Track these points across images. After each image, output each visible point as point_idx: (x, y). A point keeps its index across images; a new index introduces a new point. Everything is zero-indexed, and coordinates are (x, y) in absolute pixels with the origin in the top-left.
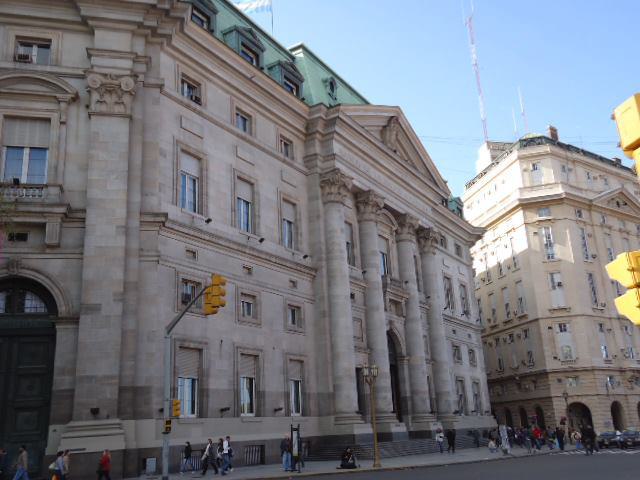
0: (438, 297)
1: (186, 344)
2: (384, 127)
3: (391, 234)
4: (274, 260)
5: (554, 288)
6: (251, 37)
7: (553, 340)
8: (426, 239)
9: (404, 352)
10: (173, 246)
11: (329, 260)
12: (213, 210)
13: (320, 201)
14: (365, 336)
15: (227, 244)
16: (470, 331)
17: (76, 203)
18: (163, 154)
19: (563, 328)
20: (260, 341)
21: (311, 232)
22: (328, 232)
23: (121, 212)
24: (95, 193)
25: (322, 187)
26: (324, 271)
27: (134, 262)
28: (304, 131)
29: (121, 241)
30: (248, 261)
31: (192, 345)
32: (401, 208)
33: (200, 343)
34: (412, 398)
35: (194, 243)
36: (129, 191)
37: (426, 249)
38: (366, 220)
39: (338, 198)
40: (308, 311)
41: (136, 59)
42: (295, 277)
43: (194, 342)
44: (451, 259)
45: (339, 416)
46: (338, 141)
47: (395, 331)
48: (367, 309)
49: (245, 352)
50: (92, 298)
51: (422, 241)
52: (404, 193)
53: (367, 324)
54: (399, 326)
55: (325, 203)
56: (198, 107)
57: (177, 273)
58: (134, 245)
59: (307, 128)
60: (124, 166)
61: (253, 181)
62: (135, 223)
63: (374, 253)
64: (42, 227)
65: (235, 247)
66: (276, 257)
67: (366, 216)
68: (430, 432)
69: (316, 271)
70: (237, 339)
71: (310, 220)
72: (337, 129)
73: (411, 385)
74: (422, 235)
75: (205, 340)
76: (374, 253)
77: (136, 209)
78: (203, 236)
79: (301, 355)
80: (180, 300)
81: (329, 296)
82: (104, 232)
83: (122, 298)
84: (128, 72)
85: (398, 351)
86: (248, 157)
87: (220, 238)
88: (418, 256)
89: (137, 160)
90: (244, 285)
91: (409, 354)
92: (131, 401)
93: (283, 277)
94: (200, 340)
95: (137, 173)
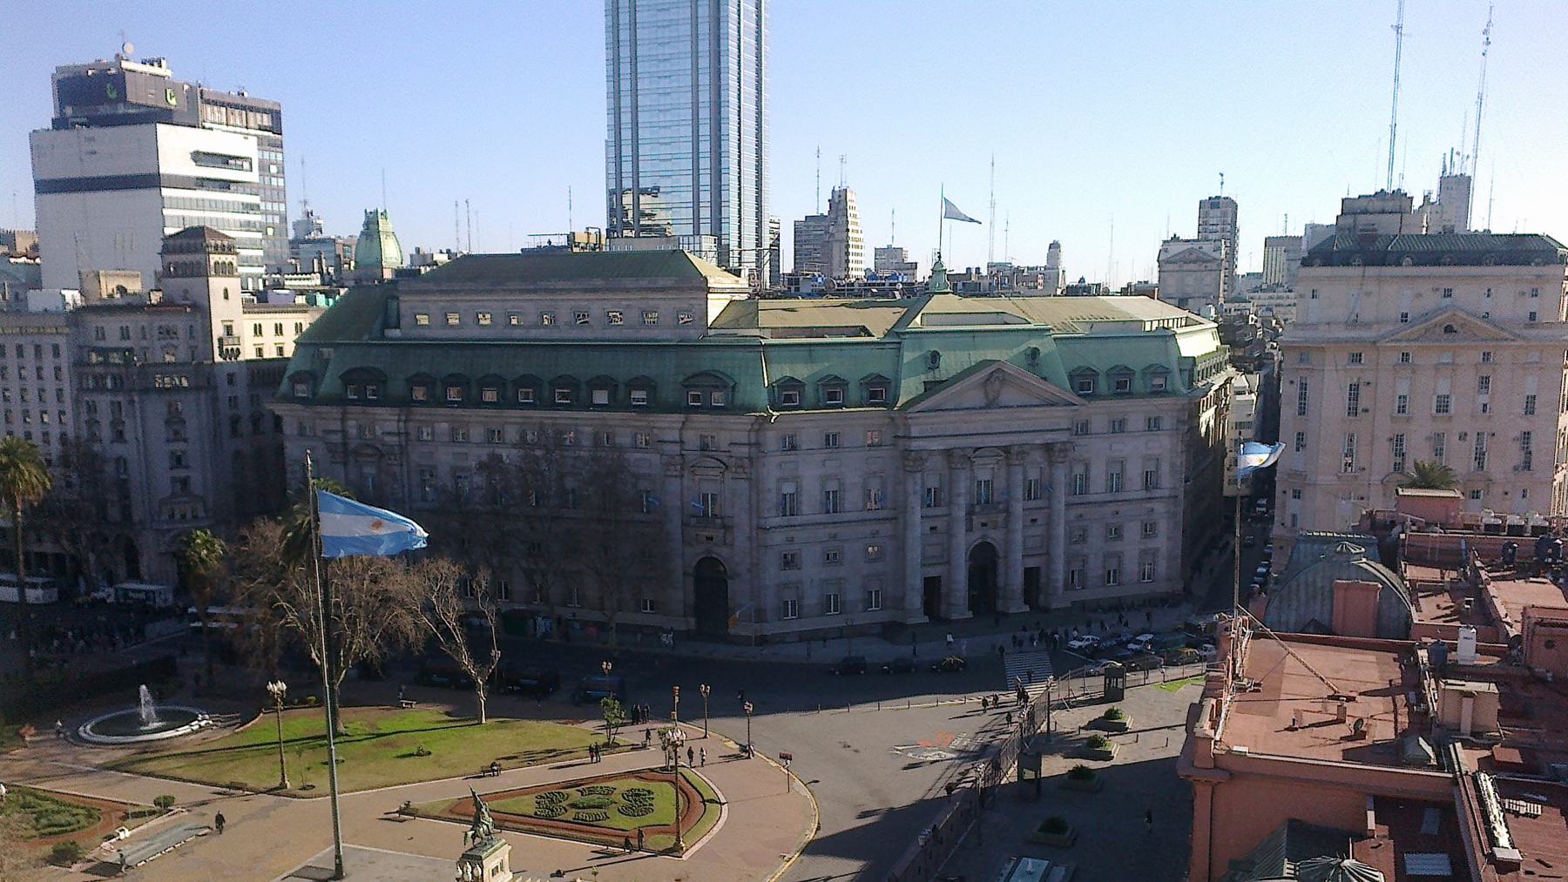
0: (1059, 502)
5: (1298, 450)
7: (1284, 505)
9: (1001, 554)
18: (770, 490)
19: (1297, 495)
29: (748, 544)
36: (750, 519)
42: (877, 527)
54: (995, 536)
55: (905, 471)
60: (747, 506)
76: (958, 495)
82: (741, 538)
83: (749, 571)
88: (1045, 465)
89: (754, 501)
91: (1006, 557)
92: (760, 615)
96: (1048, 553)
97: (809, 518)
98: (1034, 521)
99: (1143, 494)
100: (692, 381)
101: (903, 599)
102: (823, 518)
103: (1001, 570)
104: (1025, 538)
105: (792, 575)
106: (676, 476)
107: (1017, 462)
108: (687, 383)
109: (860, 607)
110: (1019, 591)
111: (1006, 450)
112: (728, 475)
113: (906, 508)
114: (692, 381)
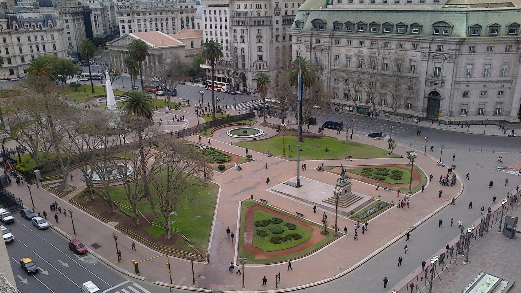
10: (463, 86)
11: (517, 79)
17: (444, 78)
18: (461, 67)
20: (486, 101)
23: (451, 82)
24: (447, 78)
26: (514, 82)
27: (452, 91)
40: (507, 92)
41: (456, 50)
50: (445, 97)
56: (473, 53)
57: (463, 91)
58: (453, 88)
62: (453, 83)
64: (438, 84)
70: (479, 101)
77: (454, 81)
81: (514, 89)
84: (455, 54)
86: (490, 58)
89: (455, 71)
92: (451, 114)
93: (499, 85)
95: (455, 74)
97: (477, 79)
100: (436, 25)
101: (510, 112)
102: (482, 79)
105: (466, 100)
106: (426, 61)
108: (434, 25)
109: (492, 114)
112: (446, 61)
113: (517, 76)
114: (436, 25)
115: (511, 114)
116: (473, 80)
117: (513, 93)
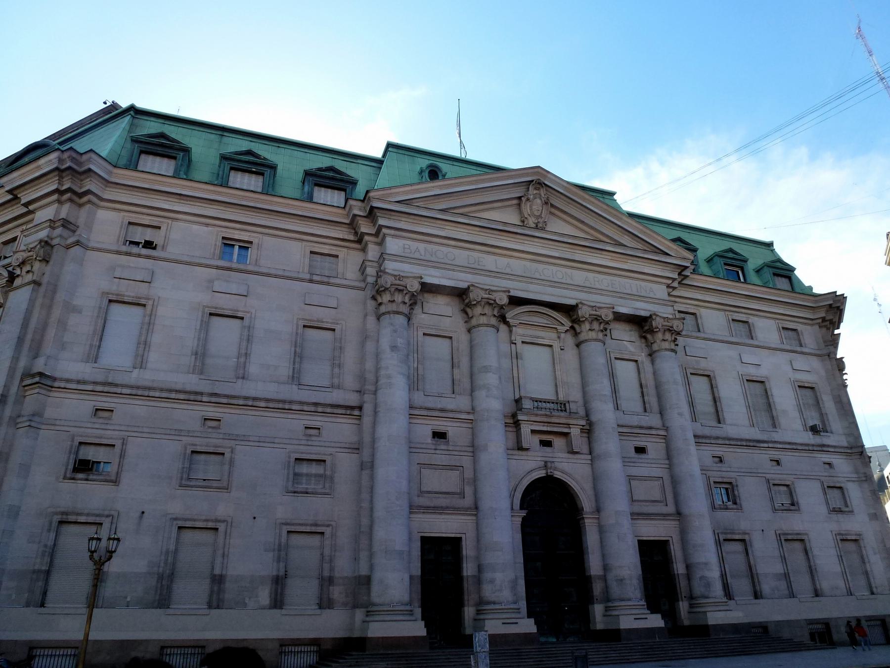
0: (680, 414)
1: (72, 518)
2: (520, 198)
3: (559, 337)
4: (263, 404)
6: (252, 159)
8: (652, 331)
9: (586, 502)
11: (375, 393)
12: (153, 357)
13: (371, 319)
14: (469, 491)
15: (164, 395)
16: (826, 458)
18: (77, 310)
20: (222, 511)
21: (362, 359)
22: (377, 357)
25: (374, 298)
26: (368, 408)
28: (352, 237)
30: (212, 411)
31: (82, 519)
32: (567, 298)
33: (97, 515)
34: (604, 578)
35: (104, 399)
37: (655, 347)
38: (474, 327)
39: (393, 307)
42: (317, 421)
43: (88, 515)
44: (765, 352)
45: (370, 610)
46: (393, 236)
47: (558, 475)
48: (474, 449)
49: (188, 524)
51: (649, 336)
52: (579, 277)
53: (475, 470)
59: (356, 233)
61: (240, 314)
63: (486, 369)
65: (182, 396)
66: (267, 400)
67: (474, 322)
68: (618, 631)
69: (360, 408)
70: (176, 508)
71: (363, 344)
72: (381, 222)
73: (604, 556)
74: (646, 328)
75: (106, 513)
76: (486, 369)
78: (119, 390)
79: (316, 525)
80: (71, 467)
81: (374, 441)
85: (579, 506)
87: (150, 389)
88: (642, 357)
90: (197, 441)
94: (97, 512)
96: (679, 513)
98: (640, 450)
99: (809, 438)
101: (366, 581)
102: (191, 382)
103: (591, 538)
104: (630, 478)
107: (593, 335)
109: (264, 596)
110: (635, 582)
111: (569, 310)
115: (377, 594)
116: (140, 383)
117: (368, 466)
